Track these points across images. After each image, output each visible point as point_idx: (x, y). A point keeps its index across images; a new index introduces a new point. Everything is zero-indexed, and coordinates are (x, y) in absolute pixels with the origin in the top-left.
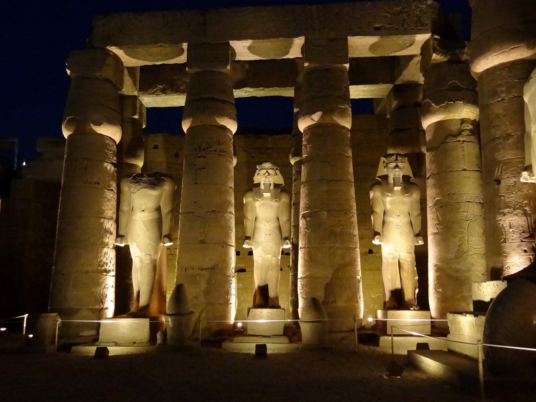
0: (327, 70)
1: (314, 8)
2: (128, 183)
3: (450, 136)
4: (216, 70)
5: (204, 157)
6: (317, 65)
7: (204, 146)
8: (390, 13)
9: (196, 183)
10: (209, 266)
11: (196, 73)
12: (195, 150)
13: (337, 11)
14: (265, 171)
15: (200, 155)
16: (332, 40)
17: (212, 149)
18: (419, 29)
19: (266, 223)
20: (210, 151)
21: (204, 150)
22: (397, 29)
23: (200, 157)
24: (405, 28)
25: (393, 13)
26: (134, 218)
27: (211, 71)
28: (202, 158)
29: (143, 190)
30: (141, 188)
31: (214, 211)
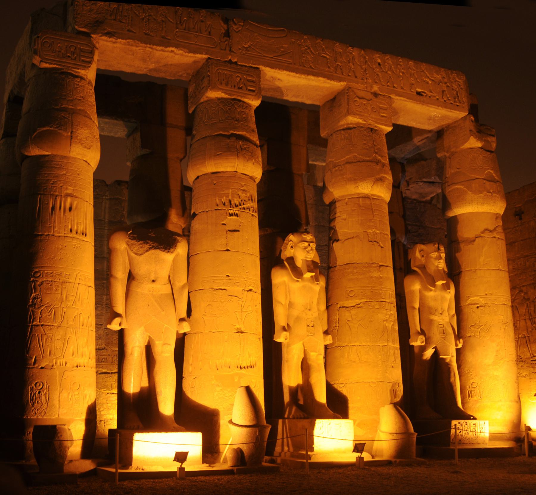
0: (372, 129)
1: (355, 52)
2: (127, 240)
3: (487, 230)
4: (246, 100)
5: (237, 215)
6: (361, 121)
7: (236, 201)
8: (430, 79)
9: (228, 250)
10: (249, 365)
11: (219, 99)
12: (224, 204)
13: (379, 61)
14: (306, 244)
15: (231, 212)
16: (376, 95)
17: (245, 206)
18: (457, 106)
19: (307, 312)
20: (244, 208)
21: (236, 206)
22: (438, 99)
23: (231, 215)
24: (445, 101)
25: (433, 80)
26: (139, 290)
27: (240, 101)
28: (234, 217)
29: (152, 251)
30: (150, 249)
31: (251, 290)
